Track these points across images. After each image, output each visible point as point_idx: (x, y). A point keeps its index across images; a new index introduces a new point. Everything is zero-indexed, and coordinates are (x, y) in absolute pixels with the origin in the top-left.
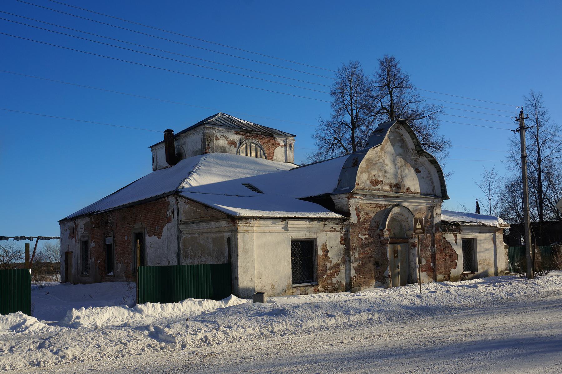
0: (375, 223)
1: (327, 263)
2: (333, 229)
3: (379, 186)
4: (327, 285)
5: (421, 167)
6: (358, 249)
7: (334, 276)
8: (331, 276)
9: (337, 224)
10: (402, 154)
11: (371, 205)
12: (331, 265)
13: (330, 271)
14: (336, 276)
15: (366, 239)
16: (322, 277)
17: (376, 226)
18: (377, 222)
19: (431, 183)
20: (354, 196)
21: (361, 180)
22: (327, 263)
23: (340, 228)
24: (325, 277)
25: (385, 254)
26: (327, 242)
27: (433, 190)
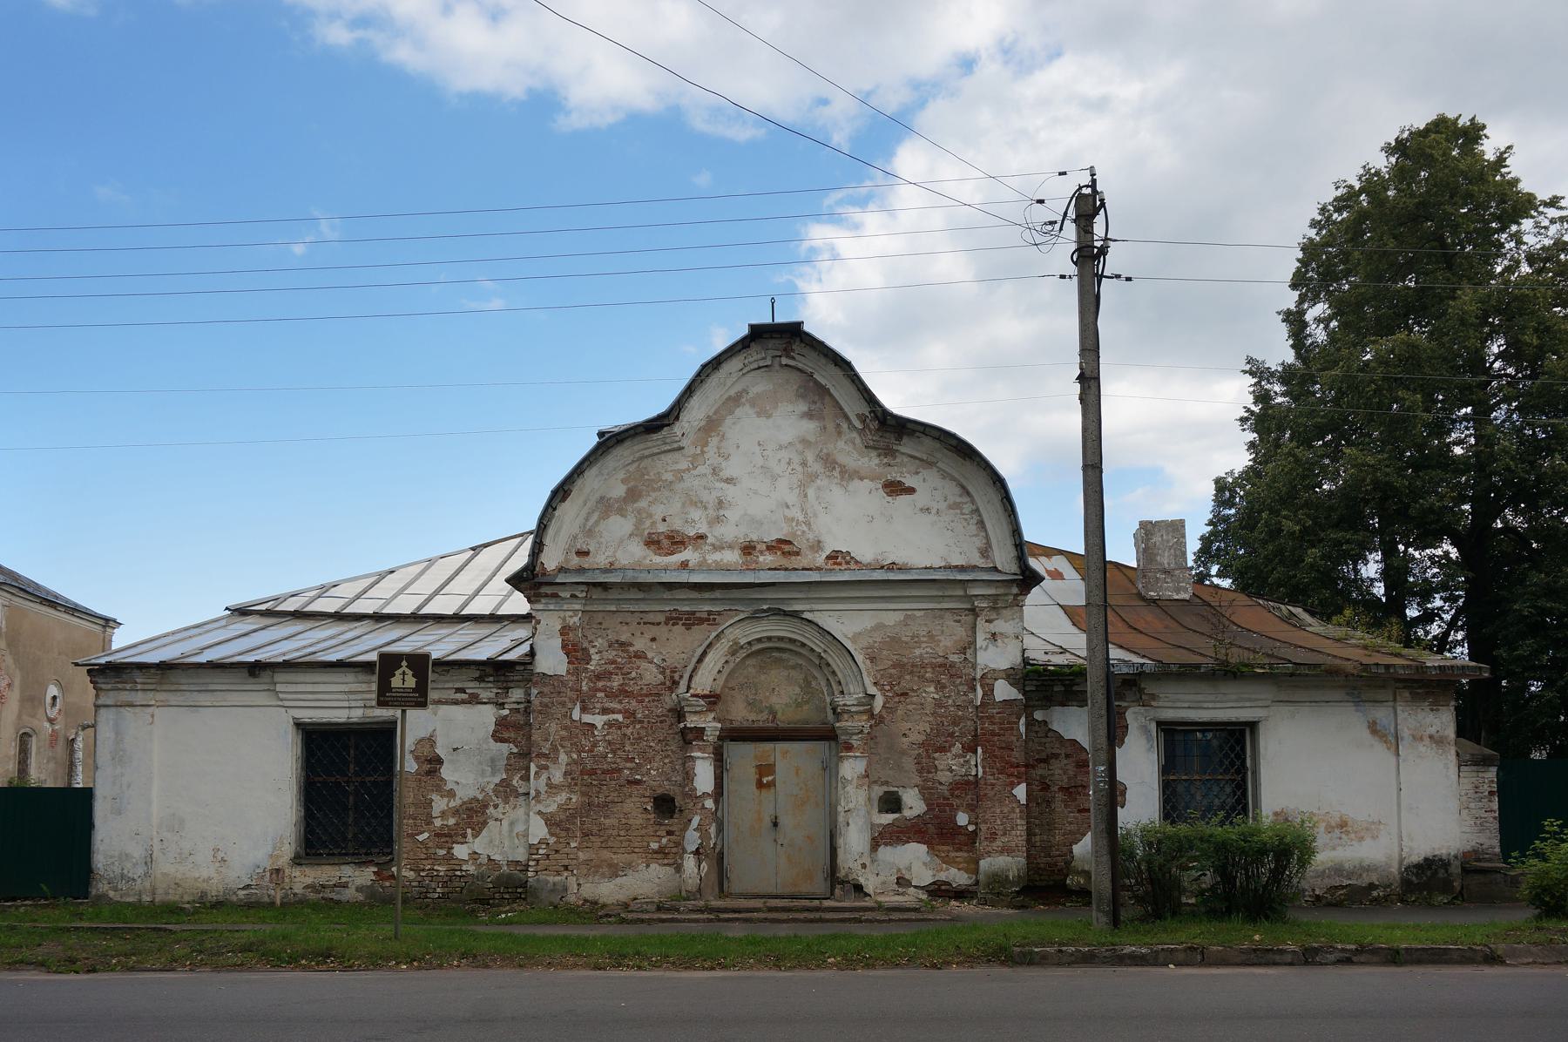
0: (663, 673)
1: (435, 797)
2: (464, 696)
3: (688, 554)
4: (430, 861)
5: (917, 473)
6: (563, 758)
7: (460, 839)
8: (448, 837)
9: (480, 679)
10: (812, 439)
11: (642, 615)
12: (452, 804)
13: (445, 823)
14: (469, 836)
15: (609, 724)
16: (412, 836)
17: (665, 684)
18: (668, 671)
19: (973, 528)
20: (544, 590)
21: (602, 540)
22: (435, 797)
23: (495, 691)
24: (421, 838)
25: (689, 776)
26: (438, 732)
27: (985, 552)
